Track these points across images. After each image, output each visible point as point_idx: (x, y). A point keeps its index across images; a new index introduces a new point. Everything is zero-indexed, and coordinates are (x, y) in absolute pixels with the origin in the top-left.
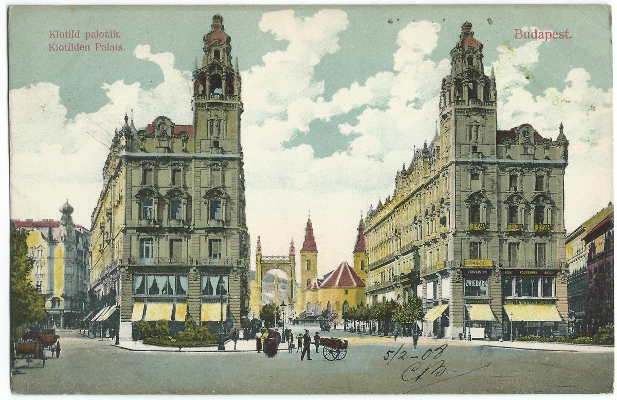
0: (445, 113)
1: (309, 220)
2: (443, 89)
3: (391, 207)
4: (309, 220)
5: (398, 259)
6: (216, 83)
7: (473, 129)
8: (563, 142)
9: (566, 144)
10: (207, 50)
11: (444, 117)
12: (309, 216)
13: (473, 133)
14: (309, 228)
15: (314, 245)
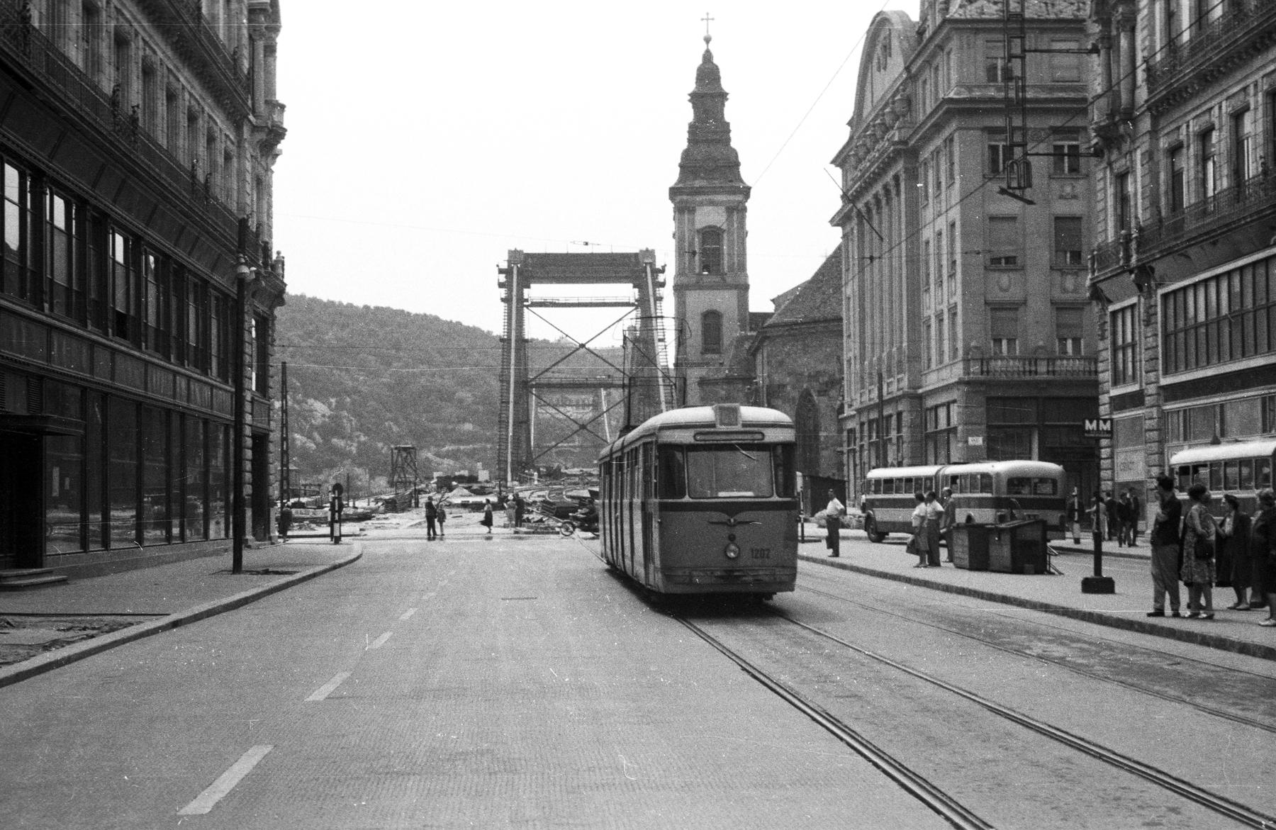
1: (708, 57)
4: (708, 57)
14: (708, 95)
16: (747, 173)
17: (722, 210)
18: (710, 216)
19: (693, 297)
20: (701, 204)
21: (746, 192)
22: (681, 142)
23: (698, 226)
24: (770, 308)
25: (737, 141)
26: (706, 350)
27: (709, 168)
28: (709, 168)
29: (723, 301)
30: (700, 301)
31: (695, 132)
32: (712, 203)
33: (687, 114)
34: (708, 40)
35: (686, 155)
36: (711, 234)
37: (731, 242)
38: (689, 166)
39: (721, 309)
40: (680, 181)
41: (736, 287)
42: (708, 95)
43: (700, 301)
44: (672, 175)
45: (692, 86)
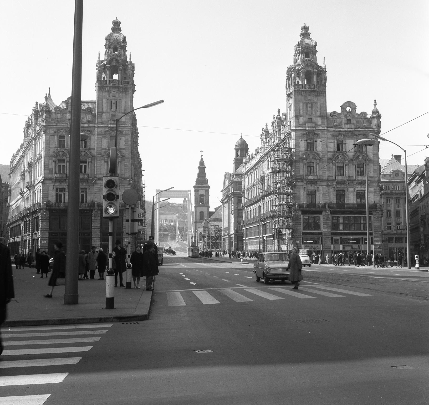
0: (288, 93)
1: (202, 159)
2: (288, 74)
3: (259, 157)
4: (202, 159)
5: (263, 199)
6: (114, 70)
7: (309, 105)
8: (377, 115)
9: (379, 116)
10: (108, 47)
11: (288, 95)
12: (202, 156)
13: (309, 109)
14: (202, 167)
15: (206, 182)
16: (209, 184)
17: (204, 191)
18: (202, 192)
19: (197, 208)
20: (200, 190)
21: (209, 187)
22: (196, 177)
23: (199, 194)
24: (214, 211)
25: (208, 177)
26: (200, 220)
27: (202, 181)
28: (202, 181)
29: (204, 209)
30: (200, 209)
31: (199, 174)
32: (202, 190)
33: (197, 171)
34: (202, 156)
35: (197, 179)
36: (202, 196)
37: (206, 197)
38: (198, 182)
39: (203, 211)
40: (196, 185)
41: (207, 207)
42: (202, 167)
43: (200, 209)
44: (194, 184)
45: (198, 165)
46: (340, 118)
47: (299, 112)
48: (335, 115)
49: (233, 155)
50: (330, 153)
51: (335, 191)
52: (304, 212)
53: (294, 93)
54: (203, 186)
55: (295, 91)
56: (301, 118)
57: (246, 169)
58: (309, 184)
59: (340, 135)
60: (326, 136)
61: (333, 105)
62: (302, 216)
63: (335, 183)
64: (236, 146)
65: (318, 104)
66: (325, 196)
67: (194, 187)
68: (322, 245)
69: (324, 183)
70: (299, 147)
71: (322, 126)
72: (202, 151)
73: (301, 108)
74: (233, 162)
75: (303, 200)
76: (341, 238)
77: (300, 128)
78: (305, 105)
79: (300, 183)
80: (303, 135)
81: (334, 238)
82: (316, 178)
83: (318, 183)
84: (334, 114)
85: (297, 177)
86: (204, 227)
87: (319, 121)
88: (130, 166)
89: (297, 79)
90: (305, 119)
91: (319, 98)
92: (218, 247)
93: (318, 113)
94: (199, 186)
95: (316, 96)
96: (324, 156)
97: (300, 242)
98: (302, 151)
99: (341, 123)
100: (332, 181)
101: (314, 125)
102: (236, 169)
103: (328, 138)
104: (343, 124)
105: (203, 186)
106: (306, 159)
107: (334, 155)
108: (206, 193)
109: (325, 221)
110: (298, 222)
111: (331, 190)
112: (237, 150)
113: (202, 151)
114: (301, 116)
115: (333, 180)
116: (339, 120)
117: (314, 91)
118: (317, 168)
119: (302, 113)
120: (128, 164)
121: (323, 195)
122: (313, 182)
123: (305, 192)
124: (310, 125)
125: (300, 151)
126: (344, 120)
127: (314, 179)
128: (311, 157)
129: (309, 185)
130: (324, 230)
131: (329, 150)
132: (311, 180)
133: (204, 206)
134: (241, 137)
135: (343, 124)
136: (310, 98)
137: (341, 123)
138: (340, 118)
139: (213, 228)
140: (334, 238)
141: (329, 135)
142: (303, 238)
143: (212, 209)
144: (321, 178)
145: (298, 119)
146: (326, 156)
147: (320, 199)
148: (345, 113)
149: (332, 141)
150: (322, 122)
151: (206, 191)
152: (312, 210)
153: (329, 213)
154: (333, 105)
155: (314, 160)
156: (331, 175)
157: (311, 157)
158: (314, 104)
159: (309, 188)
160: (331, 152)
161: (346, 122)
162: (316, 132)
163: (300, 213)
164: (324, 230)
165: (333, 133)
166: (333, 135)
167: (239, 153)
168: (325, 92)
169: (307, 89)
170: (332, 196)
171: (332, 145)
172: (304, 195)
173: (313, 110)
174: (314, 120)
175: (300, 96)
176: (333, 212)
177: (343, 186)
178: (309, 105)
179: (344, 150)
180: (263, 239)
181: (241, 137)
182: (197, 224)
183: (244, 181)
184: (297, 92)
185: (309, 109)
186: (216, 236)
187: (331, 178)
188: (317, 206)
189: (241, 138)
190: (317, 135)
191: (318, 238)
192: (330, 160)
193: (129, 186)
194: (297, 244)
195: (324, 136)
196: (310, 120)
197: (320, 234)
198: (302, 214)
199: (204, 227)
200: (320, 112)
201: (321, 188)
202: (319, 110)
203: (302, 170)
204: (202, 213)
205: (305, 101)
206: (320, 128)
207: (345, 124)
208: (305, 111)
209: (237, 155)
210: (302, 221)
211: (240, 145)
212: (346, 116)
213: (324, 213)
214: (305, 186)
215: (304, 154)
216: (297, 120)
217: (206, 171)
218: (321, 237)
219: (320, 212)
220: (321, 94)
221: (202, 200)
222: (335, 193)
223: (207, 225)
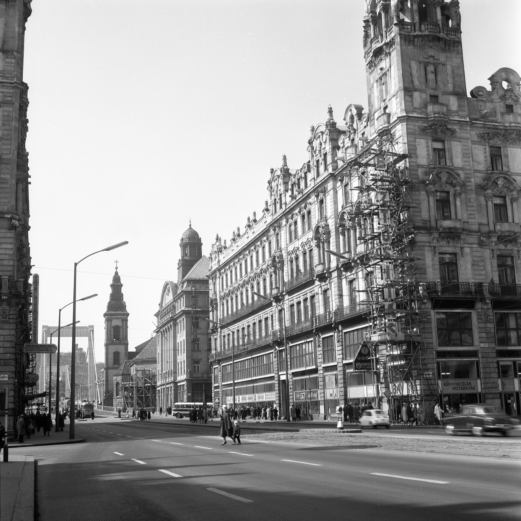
1: (116, 273)
4: (116, 273)
7: (431, 68)
13: (431, 76)
14: (117, 285)
15: (123, 307)
17: (120, 320)
18: (116, 322)
19: (110, 347)
20: (114, 318)
22: (108, 299)
23: (113, 325)
24: (134, 350)
26: (114, 364)
29: (120, 348)
30: (113, 348)
31: (112, 295)
32: (117, 318)
33: (110, 291)
34: (116, 268)
35: (109, 303)
36: (117, 329)
38: (110, 307)
39: (119, 351)
40: (108, 311)
42: (117, 285)
43: (113, 348)
44: (105, 310)
45: (111, 282)
46: (492, 101)
47: (412, 82)
48: (481, 93)
49: (177, 254)
50: (479, 175)
51: (495, 256)
52: (437, 304)
53: (398, 40)
54: (119, 312)
55: (400, 35)
56: (416, 94)
57: (219, 262)
58: (443, 238)
59: (496, 135)
60: (468, 135)
61: (477, 75)
62: (432, 311)
63: (494, 239)
64: (182, 239)
65: (449, 67)
66: (475, 268)
67: (105, 315)
68: (479, 381)
69: (474, 239)
70: (417, 157)
71: (460, 113)
72: (117, 262)
73: (414, 72)
74: (177, 266)
75: (433, 274)
76: (514, 362)
77: (415, 115)
78: (422, 65)
79: (422, 238)
80: (424, 130)
81: (501, 363)
82: (458, 225)
83: (463, 236)
84: (477, 92)
85: (417, 224)
86: (122, 375)
87: (453, 102)
88: (14, 182)
89: (402, 16)
90: (424, 96)
91: (449, 55)
92: (148, 403)
93: (450, 87)
94: (113, 312)
95: (444, 50)
96: (468, 178)
97: (433, 374)
98: (422, 166)
99: (494, 113)
100: (489, 235)
101: (445, 109)
102: (184, 276)
103: (473, 142)
104: (499, 115)
105: (119, 312)
106: (433, 182)
107: (487, 179)
108: (123, 324)
109: (482, 325)
110: (427, 326)
111: (487, 253)
112: (184, 246)
113: (117, 262)
114: (416, 90)
115: (490, 232)
116: (489, 105)
117: (439, 39)
118: (458, 203)
119: (416, 83)
120: (8, 176)
121: (473, 265)
122: (452, 235)
123: (437, 259)
124: (437, 108)
125: (419, 166)
126: (500, 107)
127: (455, 228)
128: (444, 179)
129: (443, 243)
130: (482, 345)
131: (477, 168)
132: (450, 228)
133: (120, 344)
134: (190, 226)
135: (499, 115)
136: (431, 52)
137: (494, 113)
138: (492, 101)
139: (140, 375)
140: (501, 363)
141: (474, 134)
142: (438, 363)
143: (132, 348)
144: (466, 226)
145: (411, 96)
146: (473, 180)
147: (467, 274)
148: (501, 92)
149: (481, 148)
150: (459, 106)
151: (123, 321)
152: (453, 299)
153: (490, 306)
154: (477, 75)
155: (449, 188)
156: (485, 221)
157: (444, 179)
158: (440, 67)
159: (443, 249)
160: (480, 171)
161: (503, 110)
162: (449, 127)
163: (429, 305)
164: (482, 345)
165: (481, 131)
166: (481, 137)
167: (188, 251)
168: (460, 43)
169: (427, 33)
170: (489, 268)
171: (481, 155)
172: (433, 265)
173: (439, 78)
174: (442, 99)
175: (411, 47)
176: (497, 304)
177: (509, 247)
178: (431, 68)
179: (505, 169)
180: (279, 380)
181: (190, 226)
182: (109, 371)
183: (214, 284)
184: (405, 40)
185: (431, 76)
186: (145, 387)
187: (485, 229)
188: (462, 289)
189: (191, 228)
190: (453, 132)
191: (473, 362)
192: (481, 188)
193: (9, 235)
194: (427, 379)
195: (465, 135)
196: (434, 99)
197: (474, 354)
198: (434, 307)
199: (122, 375)
200: (454, 84)
201: (467, 250)
202: (450, 80)
203: (427, 208)
204: (116, 355)
205: (421, 59)
206: (456, 118)
207: (502, 114)
208: (423, 80)
209: (184, 254)
210: (434, 324)
211: (189, 238)
212: (503, 98)
213: (479, 305)
214: (435, 243)
215: (427, 174)
216: (408, 98)
217: (123, 290)
218: (478, 362)
219: (470, 304)
220: (452, 48)
221: (117, 334)
222: (495, 262)
223: (129, 370)
